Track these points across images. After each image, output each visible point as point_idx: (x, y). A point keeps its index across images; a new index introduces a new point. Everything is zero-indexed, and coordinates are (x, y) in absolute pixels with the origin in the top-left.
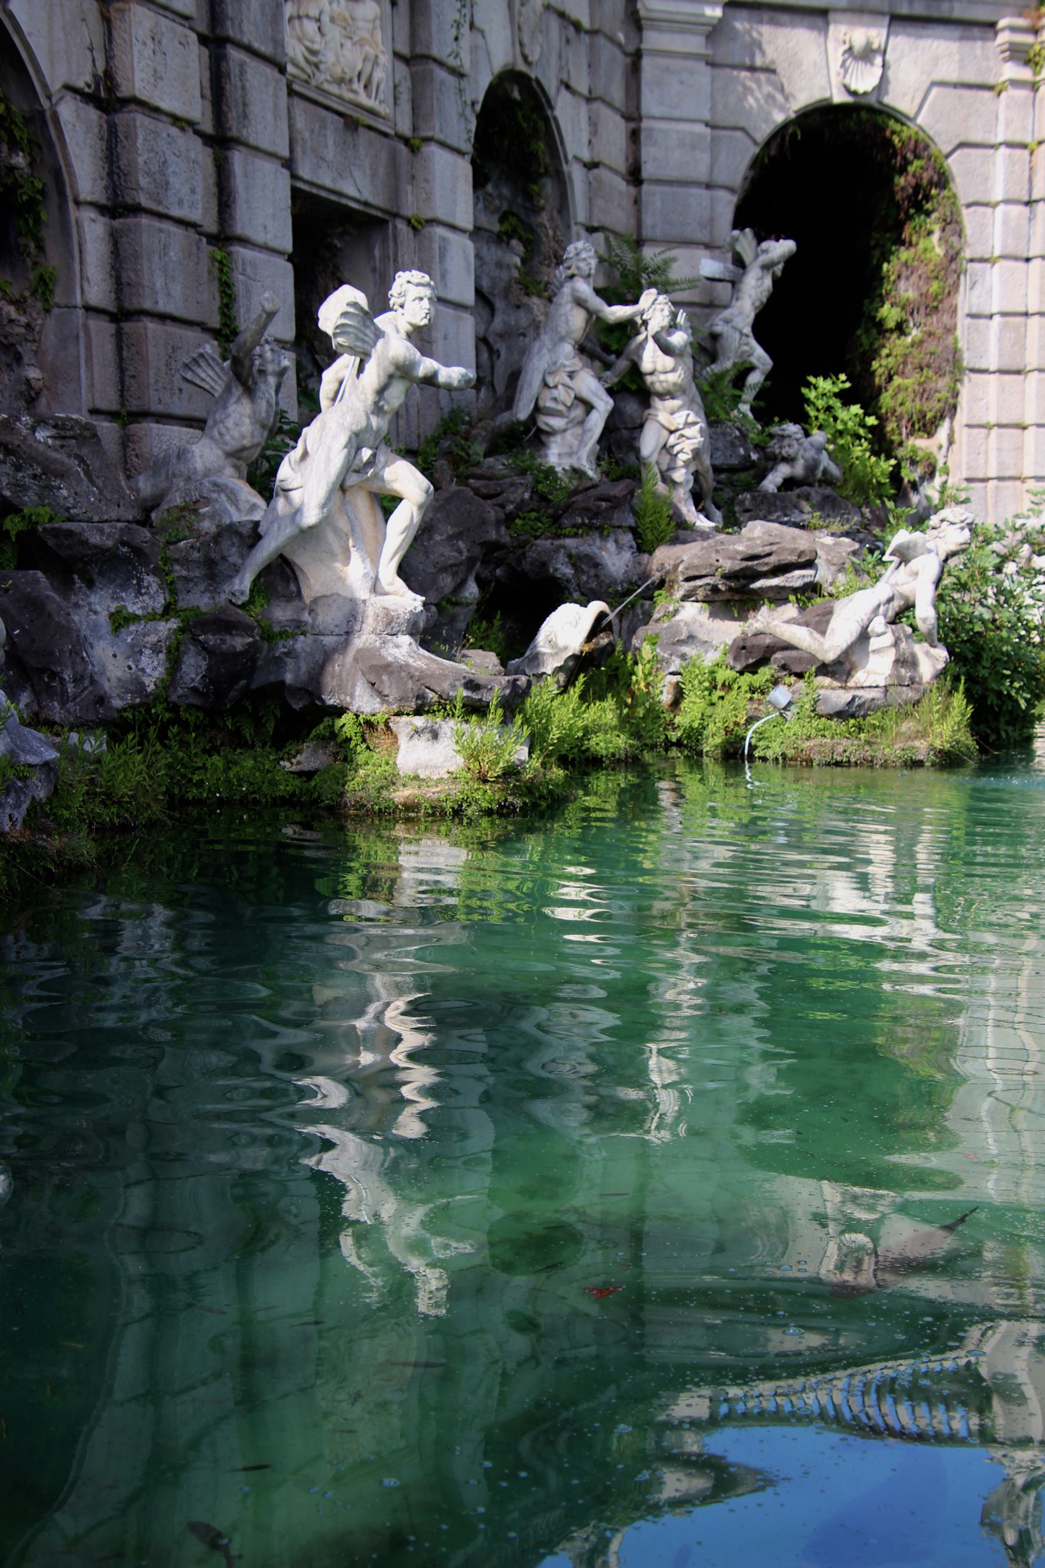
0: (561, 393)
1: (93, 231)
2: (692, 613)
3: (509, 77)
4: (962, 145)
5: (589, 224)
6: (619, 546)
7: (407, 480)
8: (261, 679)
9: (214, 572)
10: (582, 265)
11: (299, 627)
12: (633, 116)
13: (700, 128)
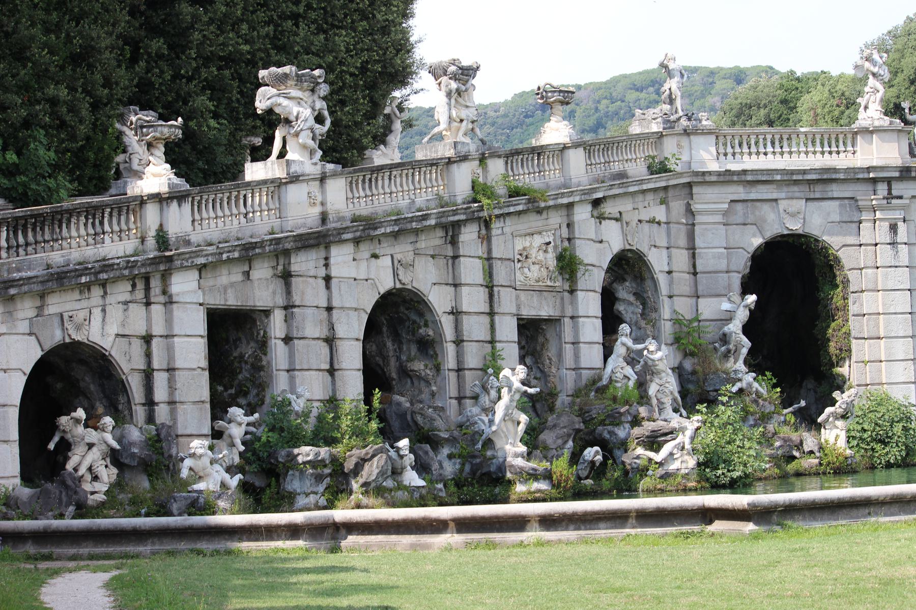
0: (618, 375)
1: (450, 349)
2: (640, 451)
3: (623, 252)
4: (844, 246)
6: (625, 428)
7: (524, 418)
8: (485, 470)
9: (474, 442)
11: (494, 457)
12: (692, 249)
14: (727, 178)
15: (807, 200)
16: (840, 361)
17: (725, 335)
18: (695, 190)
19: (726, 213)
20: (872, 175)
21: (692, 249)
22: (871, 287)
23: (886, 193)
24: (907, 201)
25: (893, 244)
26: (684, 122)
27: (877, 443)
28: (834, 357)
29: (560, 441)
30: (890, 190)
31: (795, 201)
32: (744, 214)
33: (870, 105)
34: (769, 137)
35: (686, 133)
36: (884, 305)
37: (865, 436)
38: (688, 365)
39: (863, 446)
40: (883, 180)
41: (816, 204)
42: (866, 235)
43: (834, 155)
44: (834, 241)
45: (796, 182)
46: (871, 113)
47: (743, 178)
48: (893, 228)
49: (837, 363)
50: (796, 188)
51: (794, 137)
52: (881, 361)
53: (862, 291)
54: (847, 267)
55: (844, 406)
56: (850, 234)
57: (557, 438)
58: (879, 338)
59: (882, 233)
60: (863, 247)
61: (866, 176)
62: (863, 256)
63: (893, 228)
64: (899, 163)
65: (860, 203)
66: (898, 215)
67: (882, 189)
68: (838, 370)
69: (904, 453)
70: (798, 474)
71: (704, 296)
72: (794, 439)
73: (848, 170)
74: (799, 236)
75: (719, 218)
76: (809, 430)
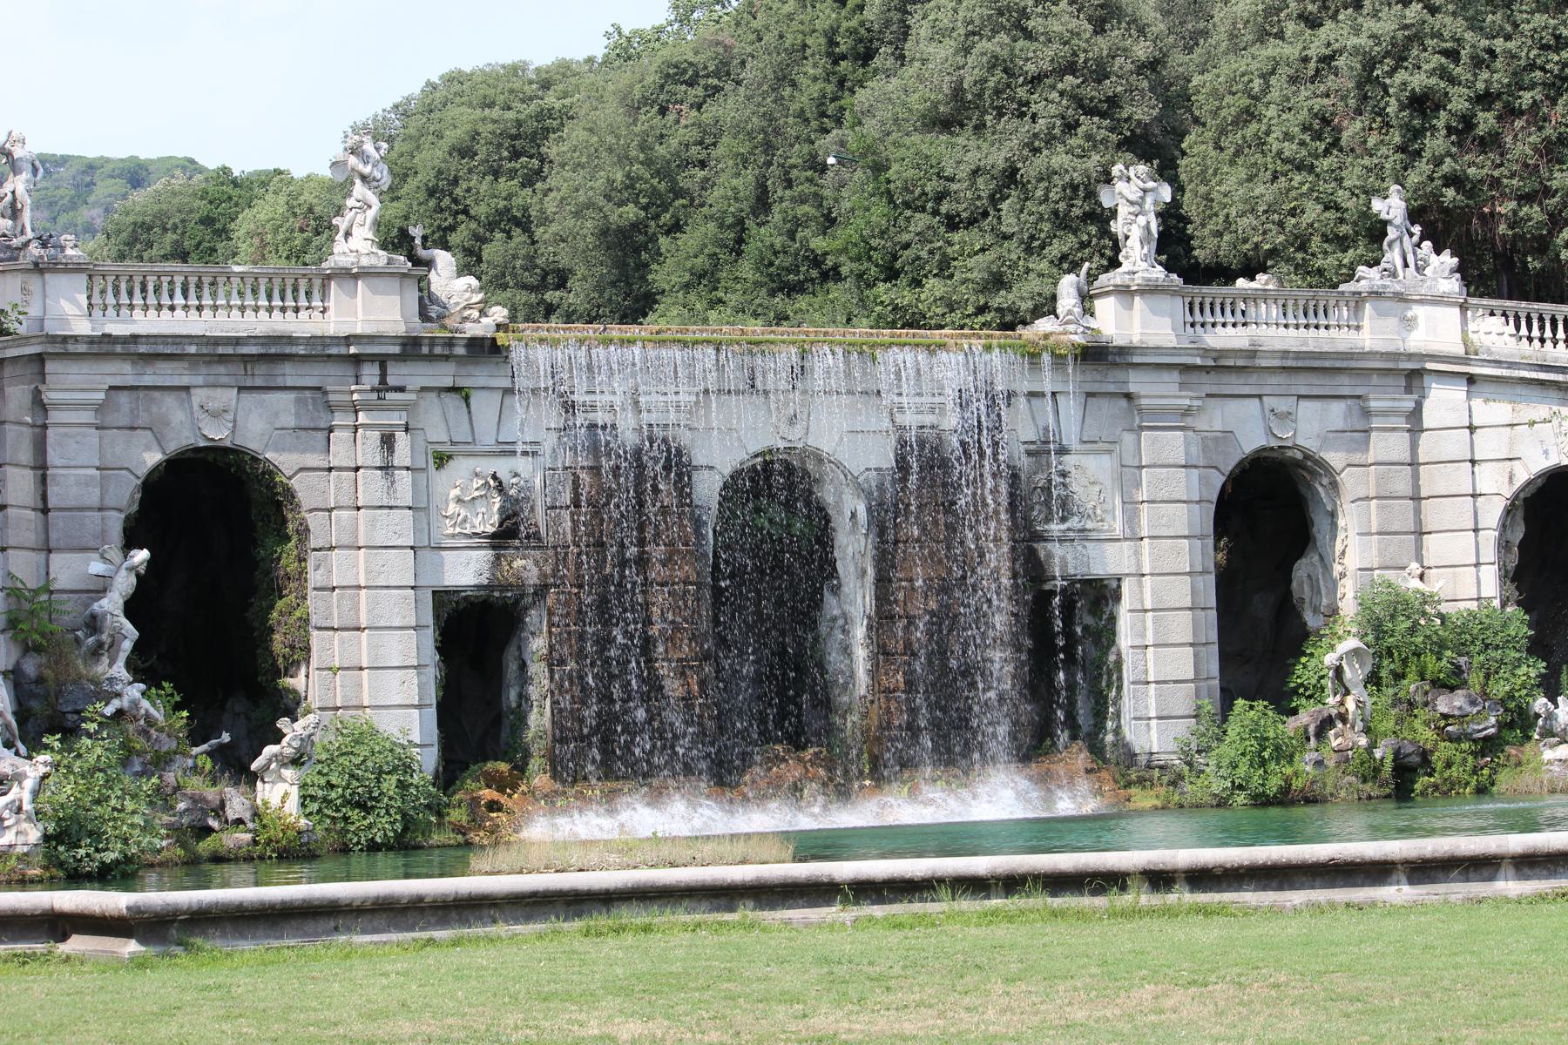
4: (301, 469)
12: (41, 468)
13: (94, 472)
14: (106, 348)
15: (241, 389)
16: (291, 667)
17: (94, 617)
18: (50, 367)
19: (100, 408)
20: (353, 350)
21: (41, 468)
22: (346, 540)
23: (376, 381)
24: (413, 396)
25: (386, 468)
26: (35, 250)
27: (352, 809)
28: (281, 660)
30: (383, 375)
31: (219, 390)
32: (132, 411)
33: (355, 231)
34: (179, 280)
35: (38, 268)
36: (368, 572)
37: (333, 795)
38: (30, 667)
39: (329, 812)
40: (371, 358)
41: (256, 396)
42: (341, 450)
43: (289, 313)
44: (284, 461)
45: (223, 359)
46: (356, 243)
47: (132, 348)
48: (388, 441)
49: (286, 669)
50: (222, 369)
51: (221, 280)
52: (361, 669)
53: (331, 548)
54: (305, 505)
55: (296, 744)
56: (313, 450)
58: (358, 629)
59: (368, 450)
60: (334, 473)
61: (343, 351)
62: (334, 489)
63: (388, 441)
64: (401, 330)
65: (331, 397)
66: (397, 419)
67: (370, 374)
68: (288, 682)
69: (399, 827)
70: (218, 859)
71: (59, 550)
72: (210, 798)
73: (312, 340)
74: (226, 450)
75: (87, 417)
76: (236, 784)
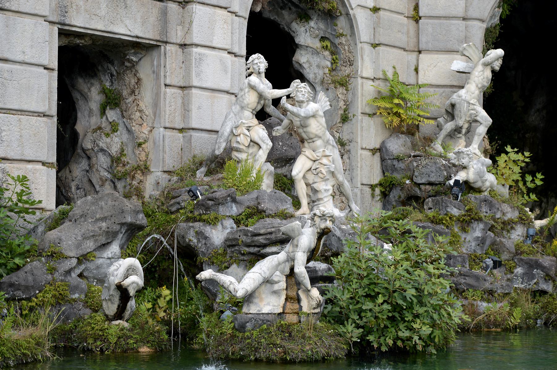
0: (241, 139)
5: (372, 42)
6: (224, 228)
10: (255, 66)
17: (453, 106)
29: (90, 245)
57: (85, 238)
71: (428, 51)
